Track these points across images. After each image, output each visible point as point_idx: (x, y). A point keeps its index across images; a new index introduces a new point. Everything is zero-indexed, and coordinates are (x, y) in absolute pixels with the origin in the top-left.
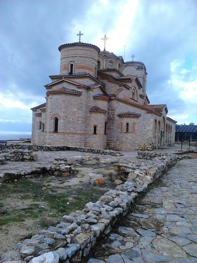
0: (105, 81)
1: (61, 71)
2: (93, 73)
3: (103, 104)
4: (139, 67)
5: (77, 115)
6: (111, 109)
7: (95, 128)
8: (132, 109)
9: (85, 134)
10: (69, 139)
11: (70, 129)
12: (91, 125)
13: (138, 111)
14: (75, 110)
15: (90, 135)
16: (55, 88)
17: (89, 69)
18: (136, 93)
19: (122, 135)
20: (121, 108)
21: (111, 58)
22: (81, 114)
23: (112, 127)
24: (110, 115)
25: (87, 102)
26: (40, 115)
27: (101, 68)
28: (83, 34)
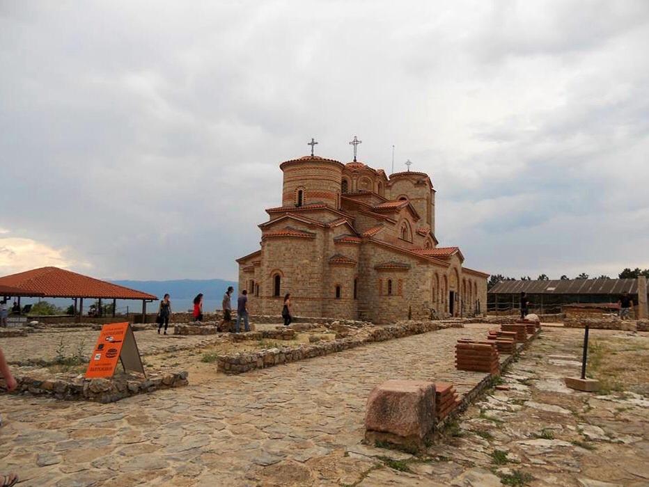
0: (355, 214)
1: (285, 199)
2: (332, 203)
3: (350, 252)
4: (418, 182)
5: (309, 270)
6: (363, 258)
7: (338, 289)
8: (396, 258)
9: (323, 299)
10: (297, 307)
11: (300, 291)
12: (331, 285)
13: (405, 260)
14: (305, 261)
15: (329, 301)
16: (275, 230)
17: (327, 196)
18: (409, 229)
19: (381, 300)
20: (379, 257)
21: (366, 174)
22: (317, 267)
23: (366, 287)
24: (362, 267)
25: (324, 249)
26: (251, 271)
27: (349, 191)
28: (317, 143)
